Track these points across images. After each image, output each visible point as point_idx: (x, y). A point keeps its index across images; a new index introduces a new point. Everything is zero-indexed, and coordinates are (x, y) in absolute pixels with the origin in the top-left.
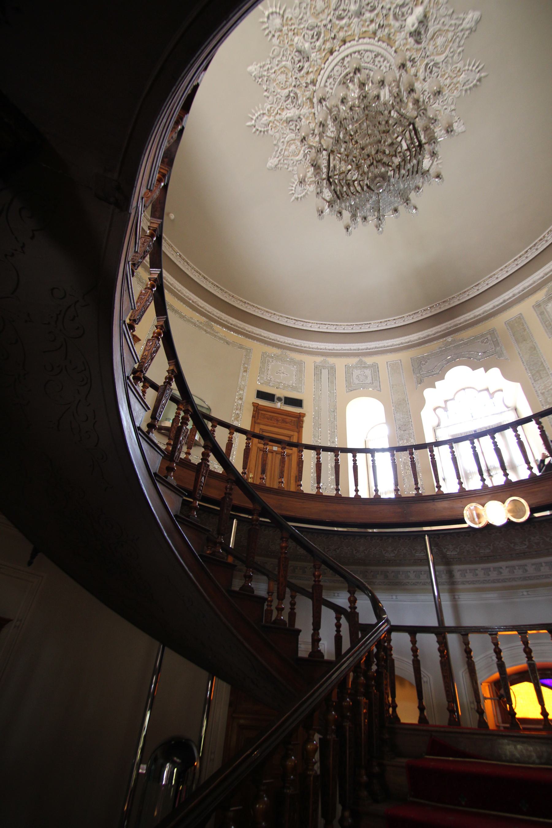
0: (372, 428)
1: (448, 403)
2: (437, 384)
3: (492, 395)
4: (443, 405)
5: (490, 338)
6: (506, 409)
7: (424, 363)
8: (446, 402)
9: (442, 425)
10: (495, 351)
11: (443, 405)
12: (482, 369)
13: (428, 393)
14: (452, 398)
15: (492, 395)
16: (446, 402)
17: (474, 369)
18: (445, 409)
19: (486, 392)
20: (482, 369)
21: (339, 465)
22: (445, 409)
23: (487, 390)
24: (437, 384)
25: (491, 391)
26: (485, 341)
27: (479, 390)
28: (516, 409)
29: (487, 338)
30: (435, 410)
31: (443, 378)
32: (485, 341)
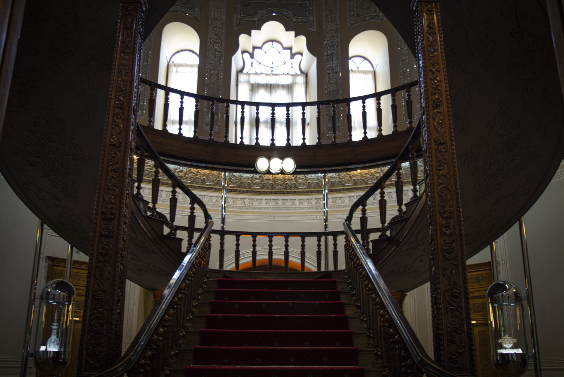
0: (178, 52)
1: (256, 50)
2: (254, 32)
3: (293, 56)
4: (251, 51)
5: (308, 5)
6: (299, 73)
7: (247, 5)
8: (254, 48)
9: (245, 71)
10: (308, 20)
11: (251, 51)
12: (293, 33)
13: (243, 38)
14: (260, 45)
15: (293, 56)
16: (254, 48)
17: (287, 29)
18: (252, 56)
19: (289, 51)
20: (293, 33)
21: (169, 104)
22: (252, 56)
23: (290, 49)
24: (254, 32)
25: (294, 51)
26: (303, 6)
27: (285, 46)
28: (306, 75)
29: (306, 3)
30: (243, 52)
31: (259, 28)
32: (303, 6)
